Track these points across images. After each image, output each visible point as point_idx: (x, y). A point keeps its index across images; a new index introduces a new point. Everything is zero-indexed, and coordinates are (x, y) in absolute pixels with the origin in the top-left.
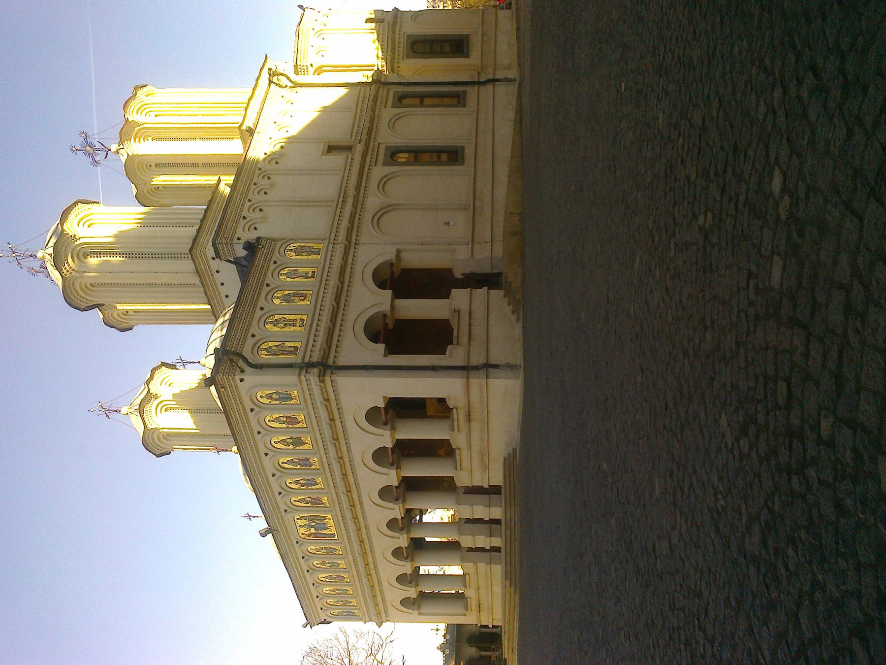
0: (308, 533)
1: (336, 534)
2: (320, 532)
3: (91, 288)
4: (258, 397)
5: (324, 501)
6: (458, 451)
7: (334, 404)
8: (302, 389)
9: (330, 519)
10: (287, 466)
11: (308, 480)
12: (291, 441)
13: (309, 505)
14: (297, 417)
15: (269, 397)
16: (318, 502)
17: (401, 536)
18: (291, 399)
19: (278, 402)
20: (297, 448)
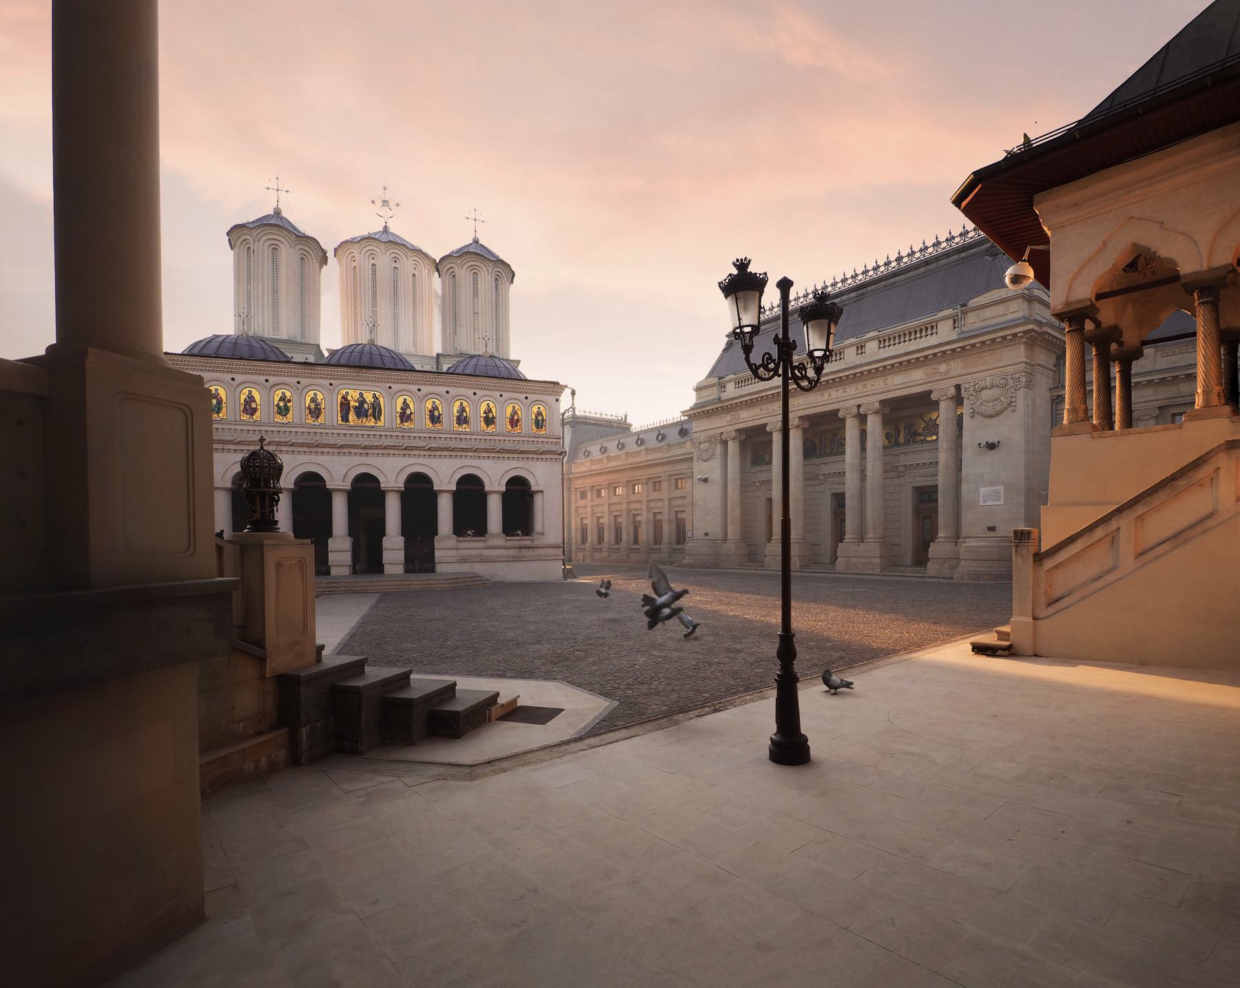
0: (349, 398)
1: (348, 423)
2: (352, 409)
3: (475, 271)
4: (539, 406)
5: (405, 424)
6: (483, 538)
7: (535, 456)
8: (550, 438)
9: (376, 423)
10: (458, 403)
11: (439, 417)
12: (491, 415)
13: (399, 410)
14: (518, 427)
15: (539, 413)
16: (405, 418)
17: (350, 484)
18: (537, 427)
19: (534, 417)
20: (482, 419)
